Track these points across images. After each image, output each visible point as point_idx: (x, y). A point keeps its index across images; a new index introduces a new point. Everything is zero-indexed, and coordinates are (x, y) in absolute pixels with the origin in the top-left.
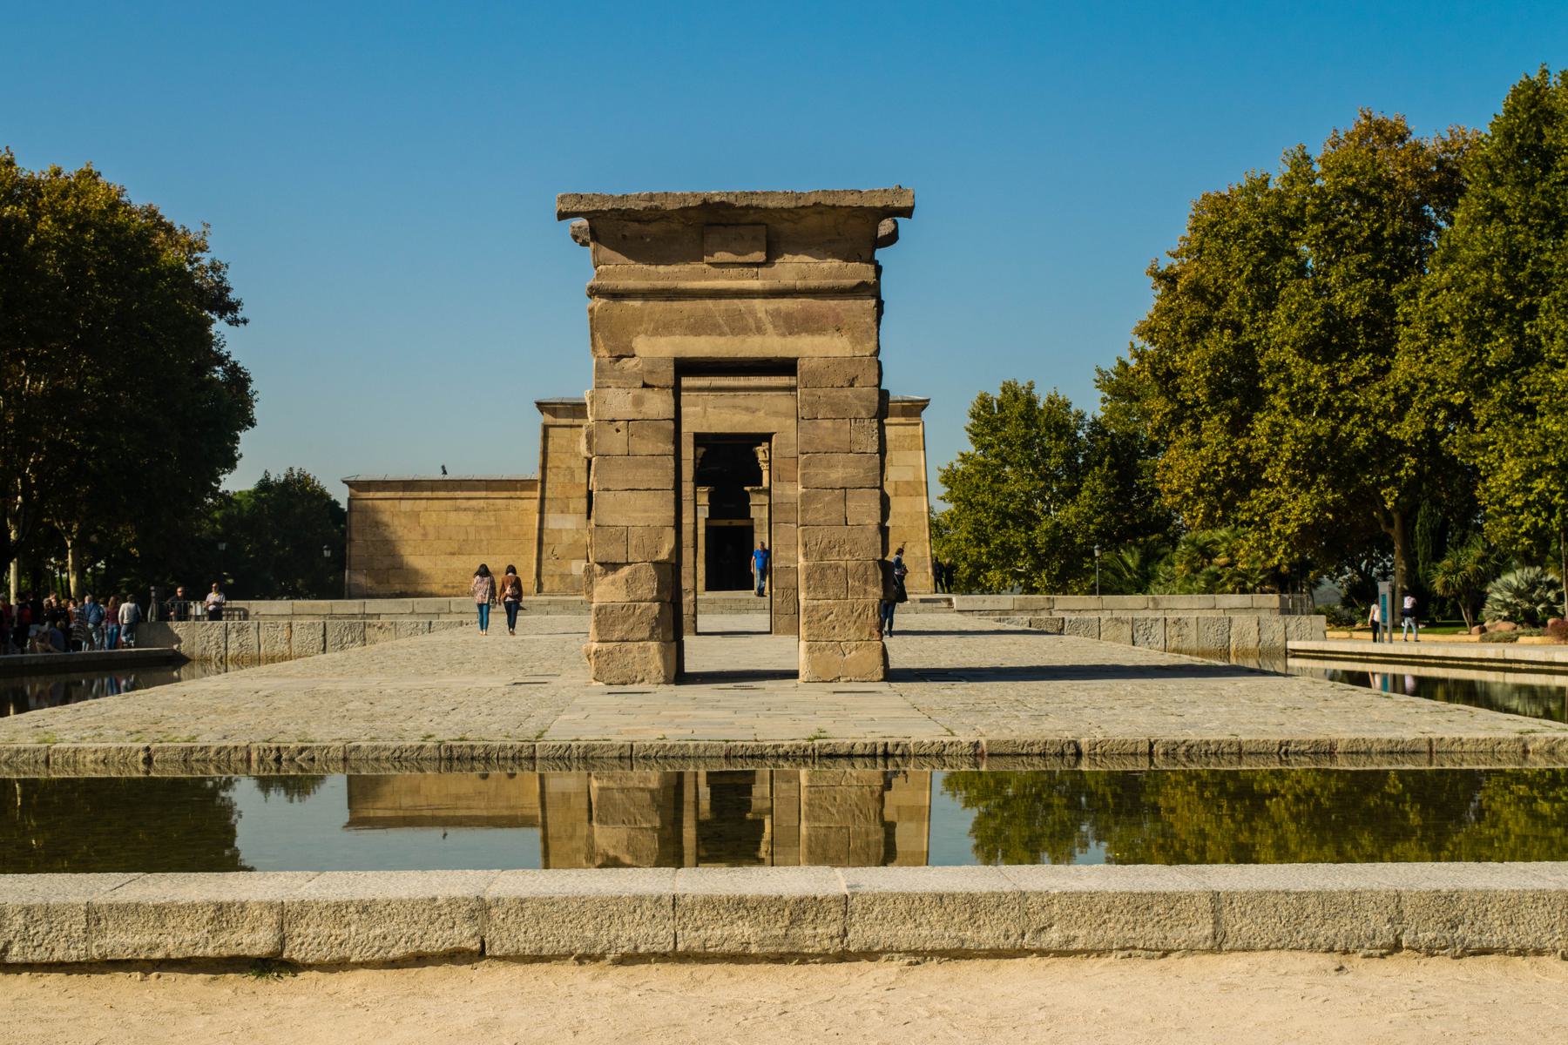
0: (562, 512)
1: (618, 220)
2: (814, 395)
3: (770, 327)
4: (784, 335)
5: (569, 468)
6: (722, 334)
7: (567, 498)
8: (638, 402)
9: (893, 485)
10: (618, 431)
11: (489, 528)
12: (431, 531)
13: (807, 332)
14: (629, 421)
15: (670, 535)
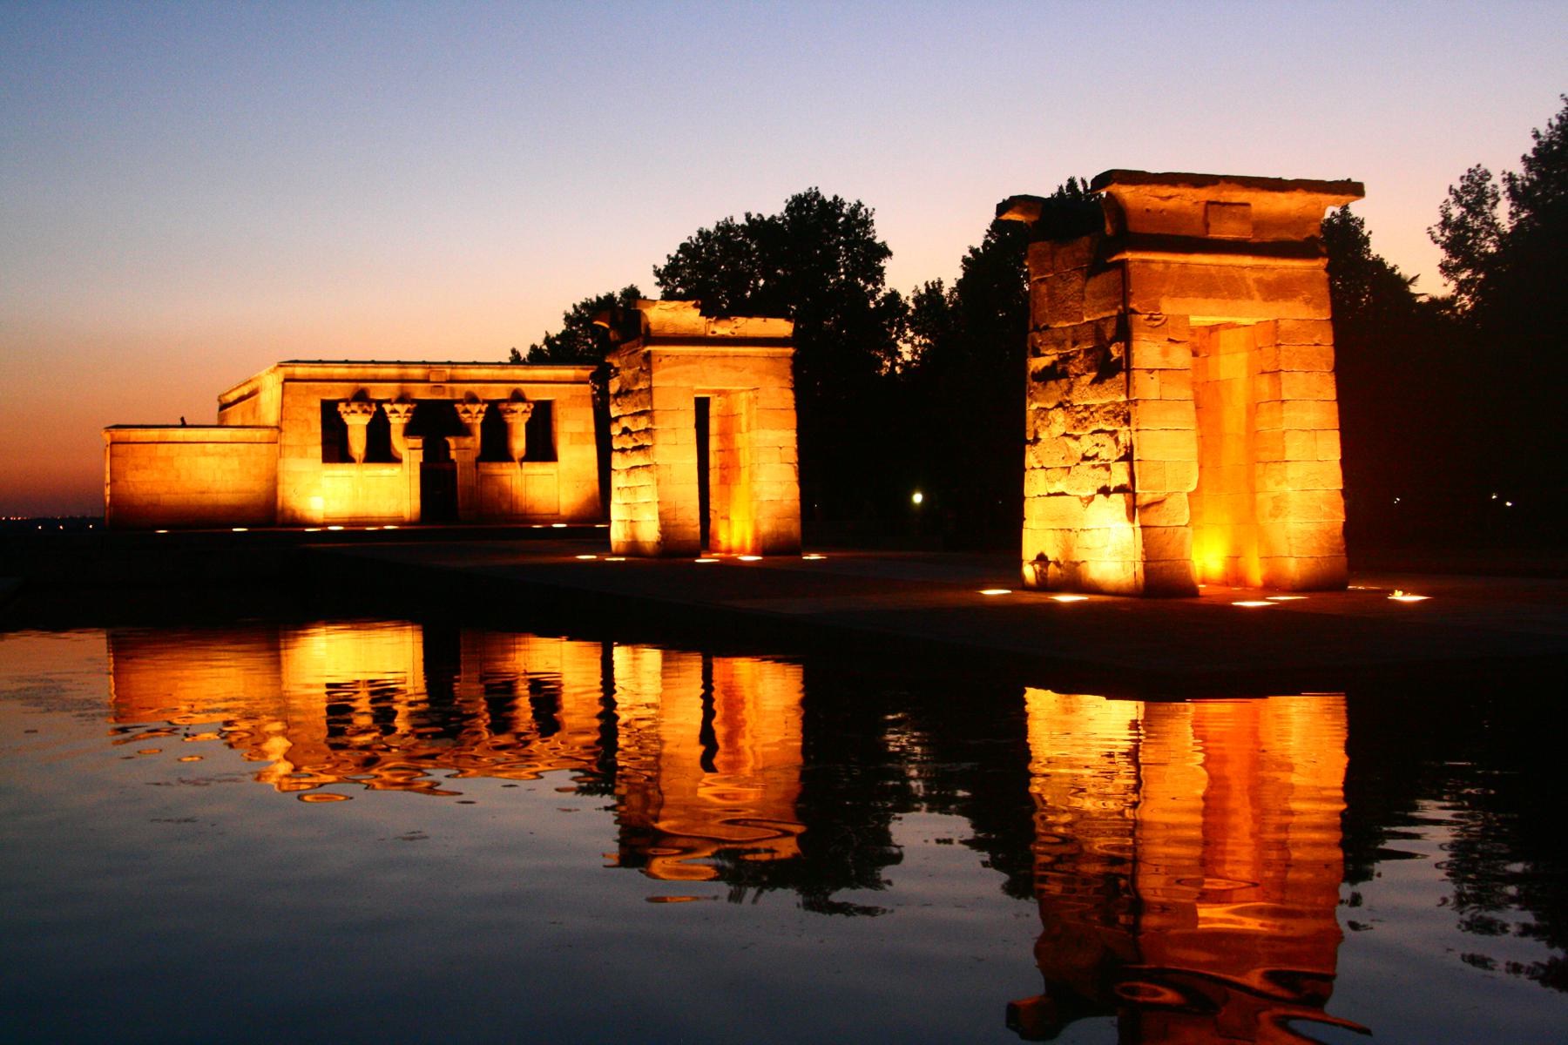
0: (302, 457)
1: (1146, 195)
2: (1289, 350)
3: (1257, 294)
4: (1265, 300)
5: (307, 421)
6: (1223, 298)
7: (305, 445)
8: (1165, 353)
9: (569, 436)
10: (1152, 378)
11: (233, 471)
12: (183, 473)
13: (1282, 298)
14: (1160, 370)
15: (1195, 467)
